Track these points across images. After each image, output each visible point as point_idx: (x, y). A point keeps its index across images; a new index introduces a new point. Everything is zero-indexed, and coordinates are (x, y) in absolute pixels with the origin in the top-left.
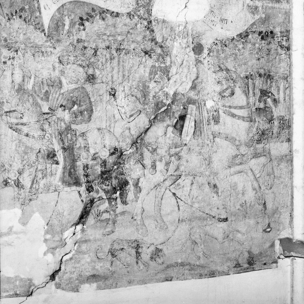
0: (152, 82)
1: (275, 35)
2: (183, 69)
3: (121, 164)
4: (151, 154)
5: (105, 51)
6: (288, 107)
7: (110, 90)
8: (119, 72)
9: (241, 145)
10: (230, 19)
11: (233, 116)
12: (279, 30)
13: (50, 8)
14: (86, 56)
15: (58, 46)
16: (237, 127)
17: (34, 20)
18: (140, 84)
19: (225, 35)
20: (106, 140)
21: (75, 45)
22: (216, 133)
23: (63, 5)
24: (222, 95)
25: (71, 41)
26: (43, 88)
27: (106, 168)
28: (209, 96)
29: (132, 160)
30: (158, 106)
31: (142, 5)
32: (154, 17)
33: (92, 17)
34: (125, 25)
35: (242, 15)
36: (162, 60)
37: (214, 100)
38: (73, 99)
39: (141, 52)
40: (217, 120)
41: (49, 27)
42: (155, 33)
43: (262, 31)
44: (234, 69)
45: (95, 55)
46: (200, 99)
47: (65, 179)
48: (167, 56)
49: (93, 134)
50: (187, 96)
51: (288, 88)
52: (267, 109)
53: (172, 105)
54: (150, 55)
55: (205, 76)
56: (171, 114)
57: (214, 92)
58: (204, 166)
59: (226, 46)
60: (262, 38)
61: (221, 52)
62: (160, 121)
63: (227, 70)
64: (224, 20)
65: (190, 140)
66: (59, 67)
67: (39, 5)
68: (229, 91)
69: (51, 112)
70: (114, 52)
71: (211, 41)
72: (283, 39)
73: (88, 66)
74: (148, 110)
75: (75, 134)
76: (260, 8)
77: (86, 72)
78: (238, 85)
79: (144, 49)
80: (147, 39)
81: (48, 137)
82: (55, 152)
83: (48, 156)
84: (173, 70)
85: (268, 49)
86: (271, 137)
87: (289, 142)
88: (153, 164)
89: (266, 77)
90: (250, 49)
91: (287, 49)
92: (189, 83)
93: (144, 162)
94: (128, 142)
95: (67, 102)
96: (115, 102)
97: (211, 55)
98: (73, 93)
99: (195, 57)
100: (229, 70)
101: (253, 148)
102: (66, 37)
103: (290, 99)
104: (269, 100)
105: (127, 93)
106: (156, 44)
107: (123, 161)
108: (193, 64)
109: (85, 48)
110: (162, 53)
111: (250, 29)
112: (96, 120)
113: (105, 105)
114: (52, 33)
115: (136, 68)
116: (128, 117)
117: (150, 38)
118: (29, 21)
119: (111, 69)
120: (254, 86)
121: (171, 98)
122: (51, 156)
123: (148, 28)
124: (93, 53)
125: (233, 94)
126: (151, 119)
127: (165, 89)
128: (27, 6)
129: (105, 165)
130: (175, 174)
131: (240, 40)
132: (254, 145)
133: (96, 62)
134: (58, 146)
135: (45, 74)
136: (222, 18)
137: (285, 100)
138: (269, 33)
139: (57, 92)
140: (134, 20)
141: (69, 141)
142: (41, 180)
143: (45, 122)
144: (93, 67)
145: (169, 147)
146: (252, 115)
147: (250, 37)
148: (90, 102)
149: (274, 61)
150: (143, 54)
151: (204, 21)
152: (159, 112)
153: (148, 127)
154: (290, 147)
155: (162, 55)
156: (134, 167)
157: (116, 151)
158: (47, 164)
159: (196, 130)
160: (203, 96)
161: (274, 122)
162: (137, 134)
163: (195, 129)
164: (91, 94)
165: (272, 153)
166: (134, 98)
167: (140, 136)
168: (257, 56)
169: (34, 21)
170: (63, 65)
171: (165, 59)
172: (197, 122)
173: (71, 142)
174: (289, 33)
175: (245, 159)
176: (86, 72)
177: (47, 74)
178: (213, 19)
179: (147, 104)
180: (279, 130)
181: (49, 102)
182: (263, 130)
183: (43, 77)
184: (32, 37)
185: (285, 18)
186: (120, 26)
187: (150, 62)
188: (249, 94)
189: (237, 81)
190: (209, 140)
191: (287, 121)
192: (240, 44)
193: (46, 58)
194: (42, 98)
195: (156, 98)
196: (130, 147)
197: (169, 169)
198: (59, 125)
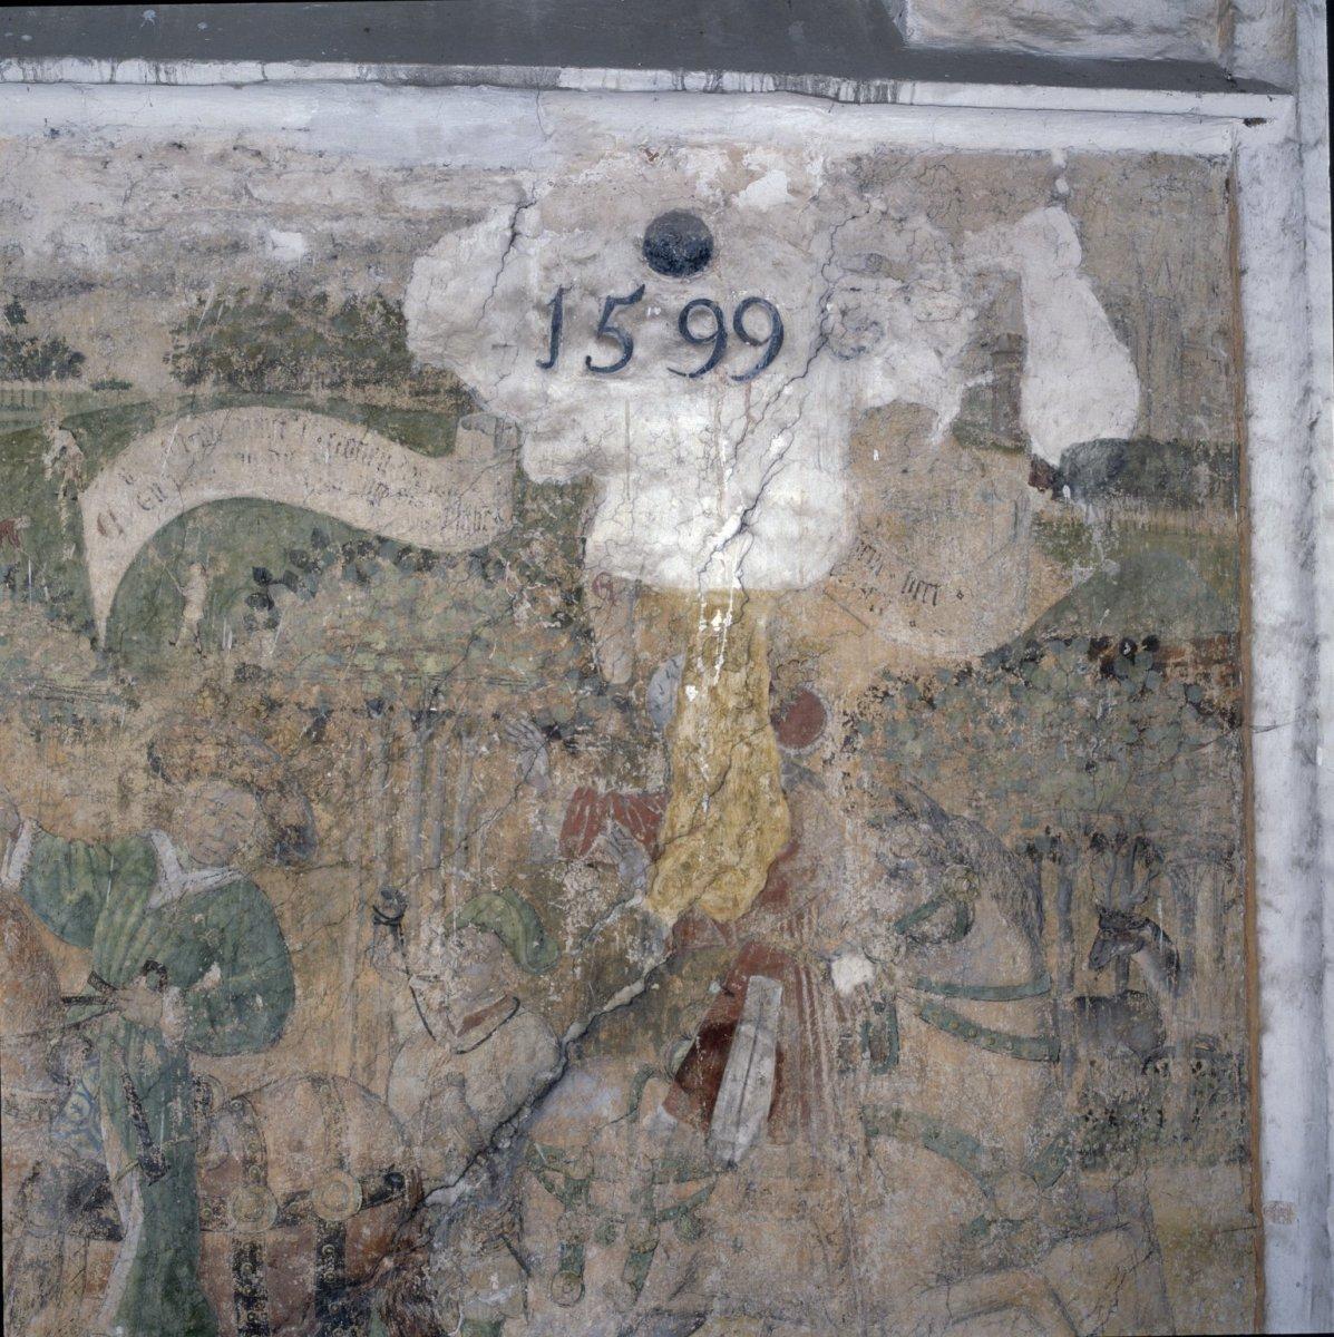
0: (578, 864)
1: (1167, 657)
2: (723, 808)
3: (414, 1250)
4: (561, 1208)
5: (362, 721)
6: (1237, 995)
7: (380, 899)
8: (422, 815)
9: (1002, 1173)
10: (953, 581)
11: (966, 1031)
12: (1191, 635)
13: (127, 529)
14: (276, 743)
15: (148, 694)
16: (985, 1083)
17: (48, 577)
18: (522, 876)
19: (925, 654)
20: (350, 1131)
21: (228, 691)
22: (882, 1113)
23: (180, 517)
24: (907, 927)
25: (207, 674)
26: (70, 882)
27: (343, 1267)
28: (848, 934)
29: (469, 1232)
30: (602, 973)
31: (539, 516)
32: (597, 572)
33: (309, 568)
34: (462, 606)
35: (1007, 564)
36: (628, 765)
37: (875, 954)
38: (206, 936)
39: (531, 727)
40: (883, 1051)
41: (113, 610)
42: (600, 643)
43: (1105, 638)
44: (966, 814)
45: (318, 740)
46: (805, 949)
47: (147, 1311)
48: (648, 747)
49: (288, 1103)
50: (743, 935)
51: (1234, 901)
52: (1130, 1002)
53: (668, 975)
54: (569, 744)
55: (833, 841)
56: (665, 1016)
57: (870, 919)
58: (818, 1273)
59: (930, 703)
60: (1107, 670)
61: (905, 734)
62: (609, 1052)
63: (937, 816)
64: (923, 588)
65: (752, 1146)
66: (147, 790)
67: (77, 514)
68: (947, 911)
69: (98, 994)
70: (404, 727)
71: (859, 681)
72: (1206, 676)
73: (281, 787)
74: (555, 998)
75: (206, 1102)
76: (1097, 535)
77: (272, 817)
78: (989, 886)
79: (541, 716)
80: (560, 670)
81: (79, 1110)
82: (107, 1178)
83: (74, 1199)
84: (681, 812)
85: (1134, 722)
86: (1156, 1140)
87: (1242, 1161)
88: (569, 1253)
89: (1124, 851)
90: (1049, 719)
91: (1231, 722)
92: (753, 872)
93: (528, 1242)
94: (451, 1145)
95: (173, 950)
96: (397, 959)
97: (859, 747)
98: (207, 909)
99: (782, 752)
100: (943, 815)
101: (1061, 1191)
102: (189, 655)
103: (1246, 954)
104: (1141, 959)
105: (455, 915)
106: (601, 693)
107: (425, 1237)
108: (771, 785)
109: (273, 705)
110: (627, 736)
111: (1046, 627)
112: (306, 1038)
113: (349, 972)
114: (126, 636)
115: (502, 800)
116: (458, 1026)
117: (571, 663)
118: (26, 581)
119: (387, 803)
120: (1069, 894)
121: (666, 942)
122: (86, 1200)
123: (567, 621)
124: (305, 730)
125: (963, 927)
126: (566, 1040)
127: (637, 901)
128: (25, 518)
129: (340, 1253)
130: (676, 1305)
131: (996, 679)
132: (1069, 1173)
133: (316, 772)
134: (120, 1156)
135: (84, 816)
136: (914, 576)
137: (1220, 958)
138: (1141, 648)
139: (131, 902)
140: (501, 586)
141: (174, 1133)
142: (32, 1311)
143: (72, 1038)
144: (305, 794)
145: (648, 1176)
146: (1057, 1029)
147: (1047, 662)
148: (285, 955)
149: (1165, 776)
150: (539, 736)
151: (830, 590)
152: (605, 1008)
153: (550, 1076)
154: (1247, 1190)
155: (627, 742)
156: (479, 1264)
157: (392, 1185)
158: (67, 1238)
159: (782, 1096)
160: (817, 934)
161: (1166, 1065)
162: (499, 1108)
163: (778, 1090)
164: (287, 915)
165: (1158, 1214)
166: (489, 938)
167: (509, 1120)
168: (1080, 752)
169: (49, 586)
170: (168, 781)
171: (641, 760)
172: (788, 1056)
173: (185, 1138)
174: (1238, 648)
175: (1022, 1241)
176: (272, 817)
177: (92, 821)
178: (871, 581)
179: (550, 969)
180: (1194, 1106)
181: (96, 947)
182: (1115, 1103)
183: (72, 833)
184: (37, 654)
185: (1219, 580)
186: (438, 610)
187: (568, 778)
188: (1041, 930)
189: (985, 868)
190: (848, 1149)
191: (1234, 1060)
192: (999, 699)
193: (90, 747)
194: (64, 928)
195: (591, 940)
196: (462, 1168)
197: (647, 1284)
198: (132, 1055)
